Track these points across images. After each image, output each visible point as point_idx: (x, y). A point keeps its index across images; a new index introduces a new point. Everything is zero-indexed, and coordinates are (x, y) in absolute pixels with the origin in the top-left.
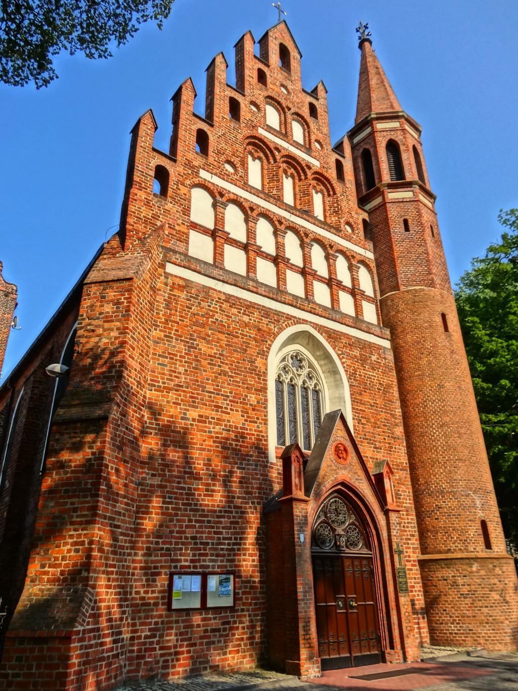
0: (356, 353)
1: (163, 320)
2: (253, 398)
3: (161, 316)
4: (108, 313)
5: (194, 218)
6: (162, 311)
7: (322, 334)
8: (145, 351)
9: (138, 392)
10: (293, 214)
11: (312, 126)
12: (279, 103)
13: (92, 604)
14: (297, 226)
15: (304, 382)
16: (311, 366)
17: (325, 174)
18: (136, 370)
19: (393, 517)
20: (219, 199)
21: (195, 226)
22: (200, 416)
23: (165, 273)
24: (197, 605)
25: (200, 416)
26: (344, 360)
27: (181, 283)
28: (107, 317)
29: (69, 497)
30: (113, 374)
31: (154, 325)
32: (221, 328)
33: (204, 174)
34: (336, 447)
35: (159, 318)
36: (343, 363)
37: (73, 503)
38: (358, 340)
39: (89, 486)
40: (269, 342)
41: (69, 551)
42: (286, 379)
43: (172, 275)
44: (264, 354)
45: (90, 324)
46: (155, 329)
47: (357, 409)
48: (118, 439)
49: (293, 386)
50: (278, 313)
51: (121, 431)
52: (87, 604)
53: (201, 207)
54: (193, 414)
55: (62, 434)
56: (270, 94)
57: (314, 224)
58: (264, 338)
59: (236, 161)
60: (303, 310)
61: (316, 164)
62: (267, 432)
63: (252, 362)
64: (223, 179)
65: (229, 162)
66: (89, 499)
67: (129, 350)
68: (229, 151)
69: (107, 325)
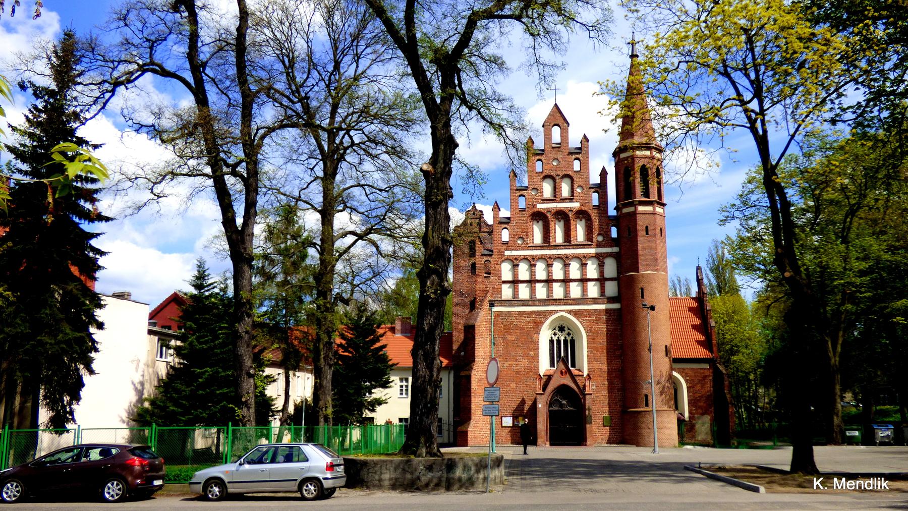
2: (532, 354)
5: (503, 279)
11: (575, 178)
17: (583, 208)
19: (587, 397)
20: (515, 263)
21: (504, 282)
32: (516, 327)
33: (507, 253)
38: (596, 310)
42: (555, 338)
44: (538, 333)
49: (559, 341)
53: (506, 271)
54: (507, 364)
58: (538, 325)
59: (523, 235)
61: (576, 205)
63: (531, 338)
68: (519, 231)
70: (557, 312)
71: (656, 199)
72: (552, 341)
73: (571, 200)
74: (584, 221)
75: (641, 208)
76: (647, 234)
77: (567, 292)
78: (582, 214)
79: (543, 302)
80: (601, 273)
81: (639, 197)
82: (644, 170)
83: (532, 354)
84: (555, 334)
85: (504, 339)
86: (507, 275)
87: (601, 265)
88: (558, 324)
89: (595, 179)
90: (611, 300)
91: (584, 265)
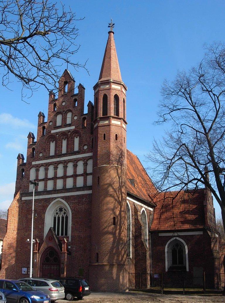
0: (76, 201)
7: (63, 200)
10: (61, 157)
11: (73, 111)
12: (61, 112)
14: (62, 161)
15: (63, 215)
16: (65, 210)
22: (28, 234)
23: (22, 201)
24: (26, 273)
25: (28, 234)
26: (71, 205)
27: (25, 201)
33: (33, 163)
34: (49, 238)
36: (70, 207)
40: (46, 209)
43: (22, 200)
44: (44, 213)
47: (74, 221)
49: (59, 218)
50: (49, 198)
56: (57, 111)
57: (69, 156)
58: (44, 208)
60: (58, 193)
61: (73, 128)
62: (43, 235)
64: (38, 161)
65: (40, 153)
70: (56, 198)
71: (112, 114)
72: (55, 218)
73: (70, 125)
74: (78, 137)
75: (101, 123)
76: (104, 139)
77: (65, 184)
78: (75, 133)
79: (50, 192)
80: (85, 170)
81: (101, 114)
82: (105, 98)
83: (40, 227)
84: (57, 214)
85: (26, 218)
86: (32, 177)
87: (85, 165)
88: (58, 206)
89: (86, 111)
90: (90, 188)
91: (75, 166)
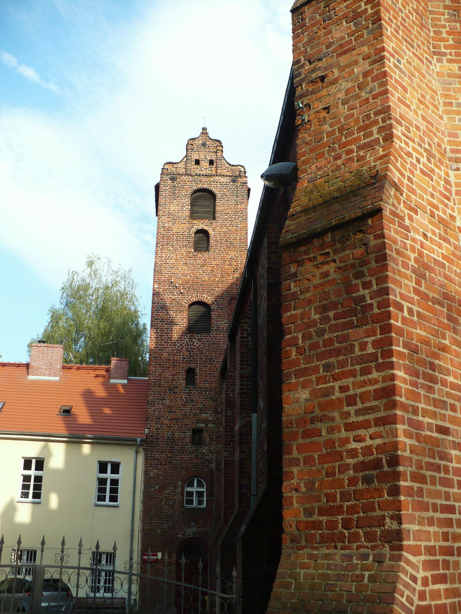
1: (451, 42)
3: (444, 35)
4: (342, 38)
6: (444, 26)
8: (428, 97)
9: (432, 171)
13: (419, 587)
18: (418, 128)
28: (341, 46)
29: (335, 378)
30: (376, 136)
31: (434, 53)
35: (443, 40)
37: (343, 389)
39: (370, 350)
41: (353, 481)
45: (313, 71)
46: (439, 61)
48: (412, 256)
51: (414, 240)
52: (407, 585)
55: (300, 264)
66: (375, 375)
67: (396, 89)
69: (343, 60)
